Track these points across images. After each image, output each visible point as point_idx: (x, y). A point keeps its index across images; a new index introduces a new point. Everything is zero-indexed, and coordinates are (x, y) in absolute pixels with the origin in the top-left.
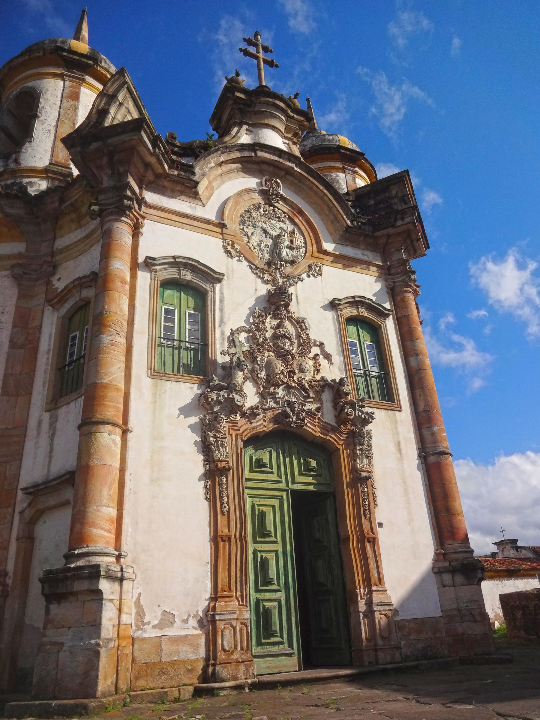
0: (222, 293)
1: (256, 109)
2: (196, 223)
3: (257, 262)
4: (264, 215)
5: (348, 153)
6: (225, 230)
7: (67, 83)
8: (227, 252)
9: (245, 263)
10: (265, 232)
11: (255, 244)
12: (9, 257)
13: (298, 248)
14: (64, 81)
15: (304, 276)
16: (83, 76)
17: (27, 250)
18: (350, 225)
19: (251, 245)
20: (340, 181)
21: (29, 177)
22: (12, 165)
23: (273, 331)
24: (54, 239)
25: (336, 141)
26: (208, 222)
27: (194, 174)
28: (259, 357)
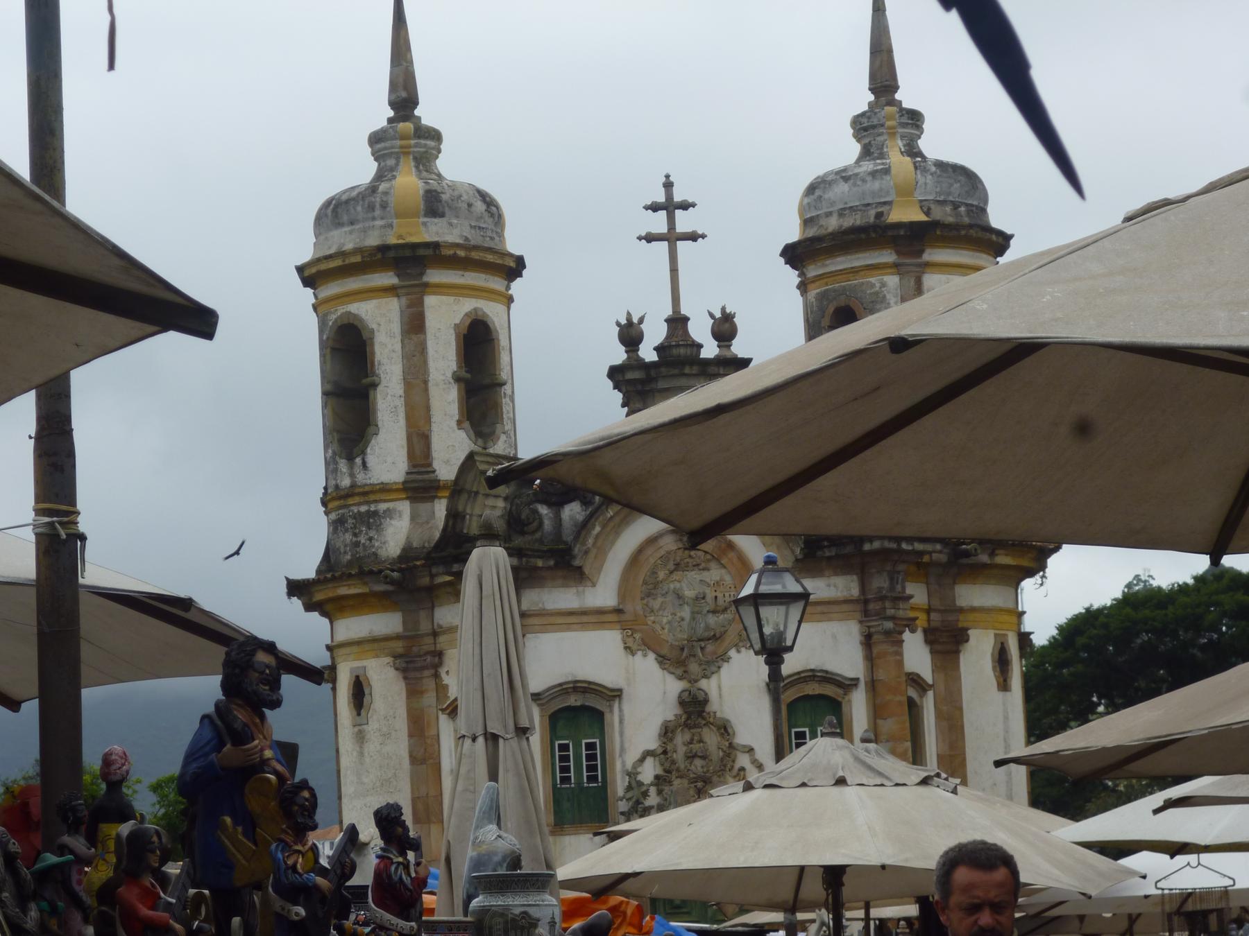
0: (621, 710)
1: (661, 384)
2: (585, 619)
3: (665, 651)
4: (676, 570)
5: (902, 233)
6: (624, 617)
7: (404, 300)
8: (626, 648)
9: (651, 656)
10: (679, 597)
11: (665, 620)
12: (387, 639)
13: (725, 610)
14: (398, 296)
15: (732, 653)
16: (422, 274)
17: (404, 623)
18: (800, 557)
19: (658, 627)
20: (888, 297)
21: (385, 501)
22: (361, 478)
23: (684, 748)
24: (433, 608)
25: (888, 193)
26: (600, 612)
27: (574, 557)
28: (667, 789)
